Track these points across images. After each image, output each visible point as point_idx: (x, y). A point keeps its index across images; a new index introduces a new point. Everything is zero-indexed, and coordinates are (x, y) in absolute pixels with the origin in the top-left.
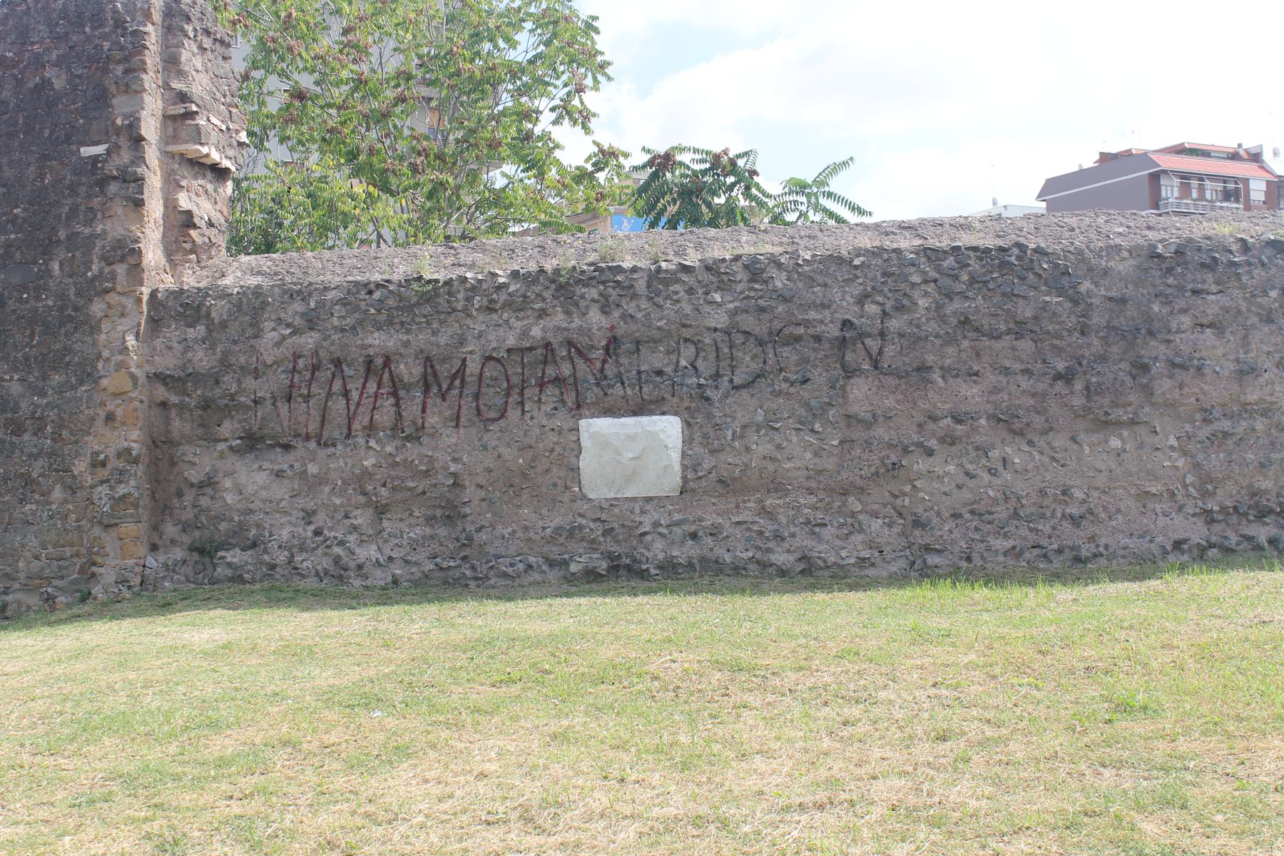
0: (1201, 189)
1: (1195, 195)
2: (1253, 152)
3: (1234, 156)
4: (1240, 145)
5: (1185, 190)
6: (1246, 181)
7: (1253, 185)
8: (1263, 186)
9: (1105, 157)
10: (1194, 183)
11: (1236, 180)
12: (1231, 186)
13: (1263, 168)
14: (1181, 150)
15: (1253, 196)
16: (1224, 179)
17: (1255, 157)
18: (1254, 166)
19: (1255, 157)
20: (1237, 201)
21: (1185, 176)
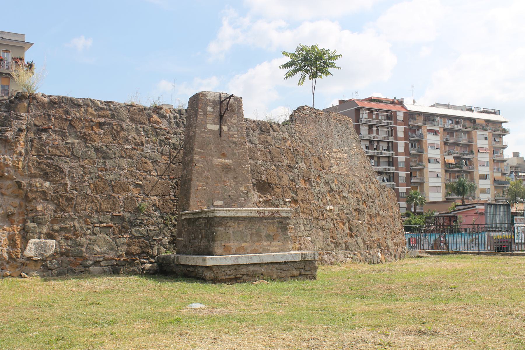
0: (377, 115)
1: (374, 117)
2: (400, 101)
3: (392, 103)
4: (395, 98)
5: (370, 115)
6: (395, 112)
7: (398, 114)
8: (402, 114)
9: (341, 102)
10: (374, 113)
11: (391, 112)
12: (389, 114)
13: (404, 107)
14: (371, 100)
15: (398, 118)
16: (387, 111)
17: (401, 103)
18: (400, 106)
19: (401, 103)
20: (391, 120)
21: (370, 110)
